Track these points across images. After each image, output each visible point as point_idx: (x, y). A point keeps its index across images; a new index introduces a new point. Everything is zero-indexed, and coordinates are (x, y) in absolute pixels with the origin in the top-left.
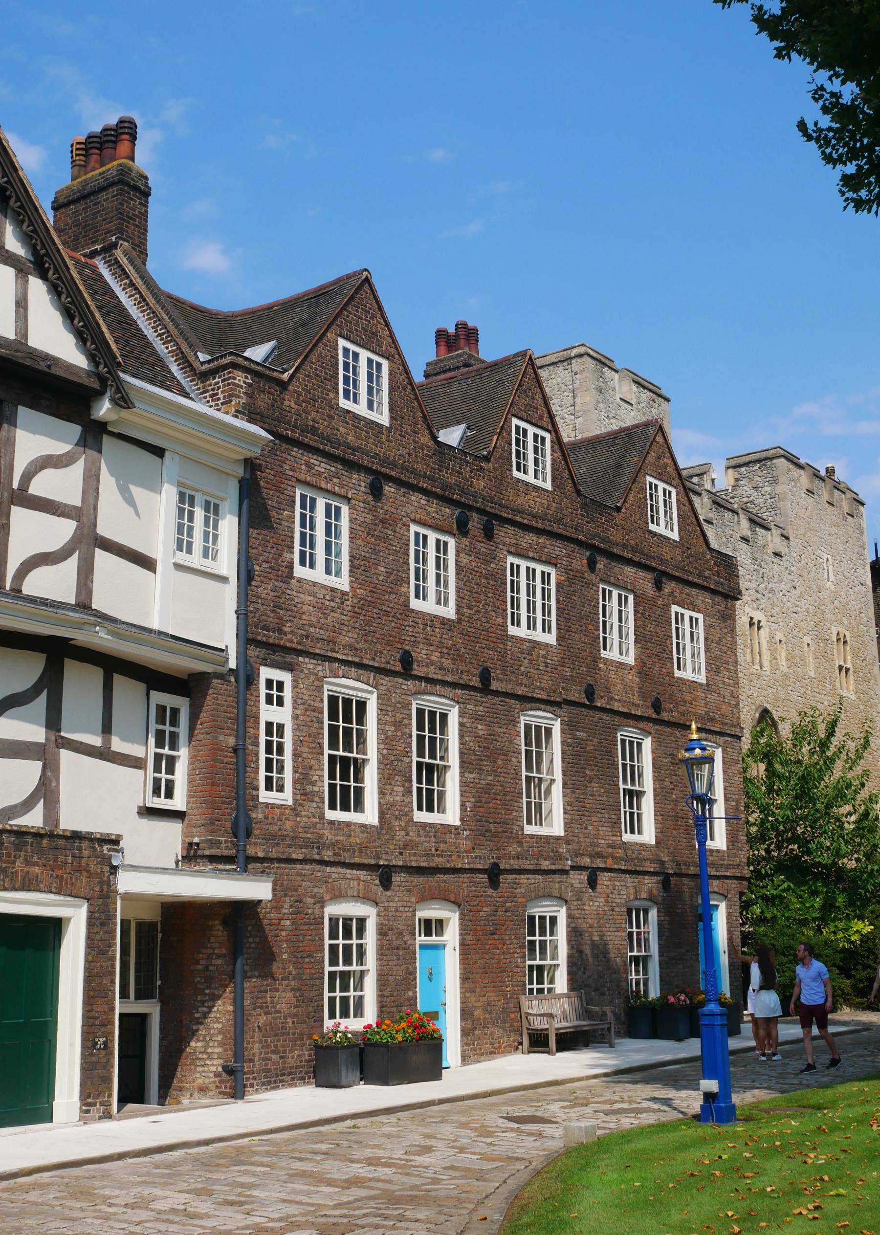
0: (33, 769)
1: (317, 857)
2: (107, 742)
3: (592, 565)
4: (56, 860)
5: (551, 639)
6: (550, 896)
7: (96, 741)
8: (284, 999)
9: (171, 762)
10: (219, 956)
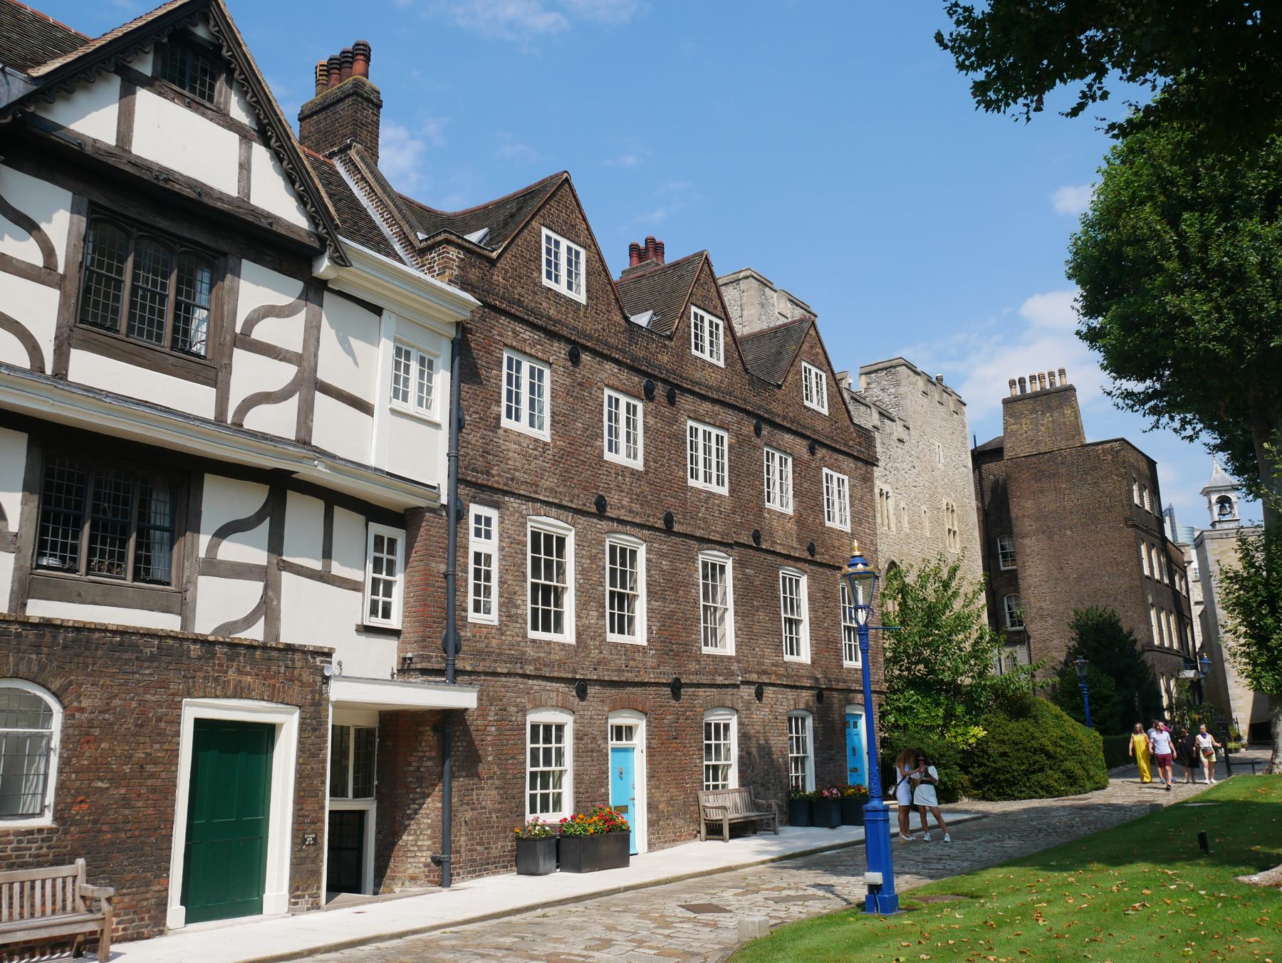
0: (253, 591)
1: (520, 671)
2: (327, 567)
3: (758, 431)
4: (269, 670)
5: (724, 491)
6: (724, 706)
7: (317, 565)
8: (488, 796)
9: (388, 586)
10: (429, 759)
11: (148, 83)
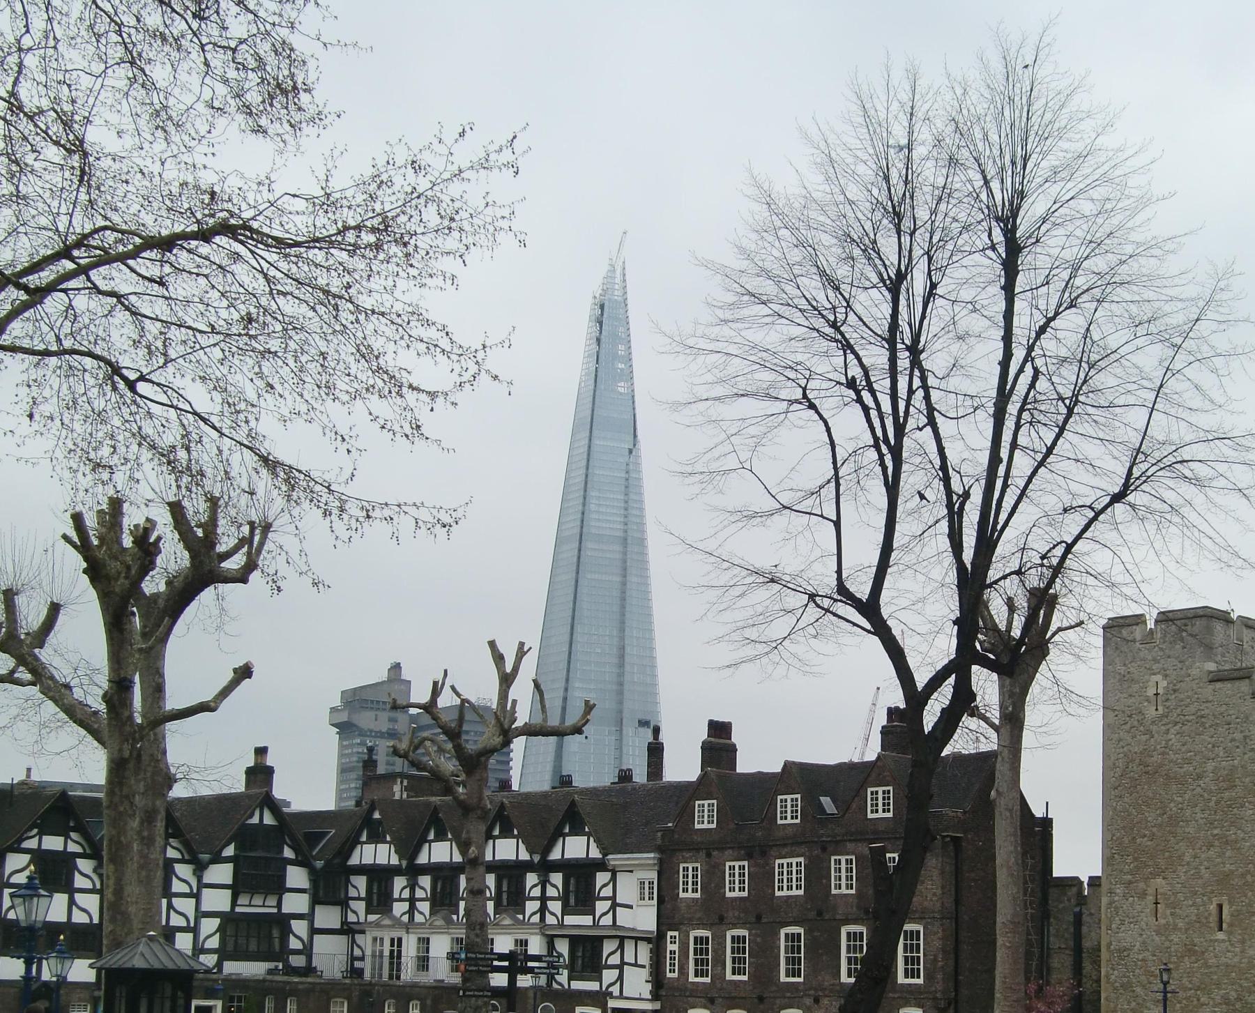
5: (801, 892)
11: (568, 835)
